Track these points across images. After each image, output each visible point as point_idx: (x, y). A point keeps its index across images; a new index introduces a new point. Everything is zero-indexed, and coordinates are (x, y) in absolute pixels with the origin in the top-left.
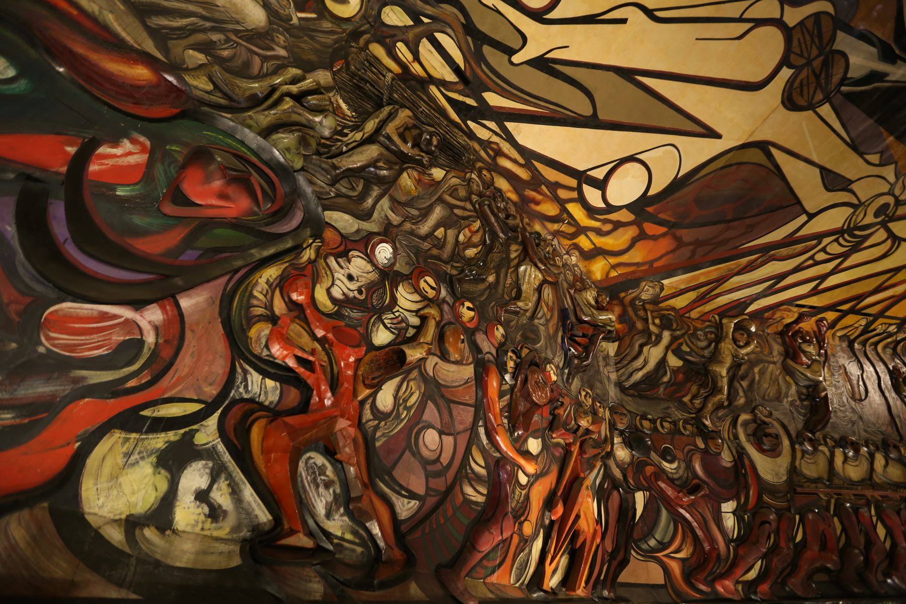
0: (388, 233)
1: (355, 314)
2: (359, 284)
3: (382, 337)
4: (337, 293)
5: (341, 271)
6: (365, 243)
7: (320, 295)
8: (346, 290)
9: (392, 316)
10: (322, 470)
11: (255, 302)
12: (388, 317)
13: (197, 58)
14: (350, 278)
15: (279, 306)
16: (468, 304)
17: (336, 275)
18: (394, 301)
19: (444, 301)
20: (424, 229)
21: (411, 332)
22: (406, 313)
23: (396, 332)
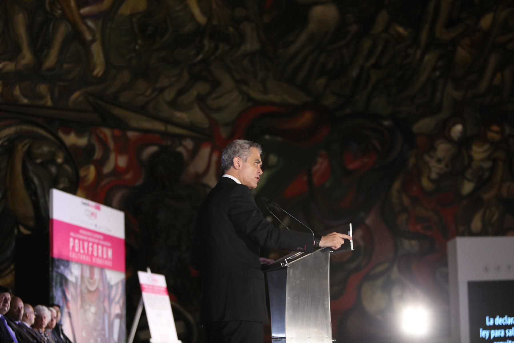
0: (457, 116)
3: (468, 187)
6: (442, 131)
7: (425, 183)
12: (468, 175)
13: (322, 81)
15: (406, 201)
18: (471, 159)
20: (484, 85)
21: (487, 174)
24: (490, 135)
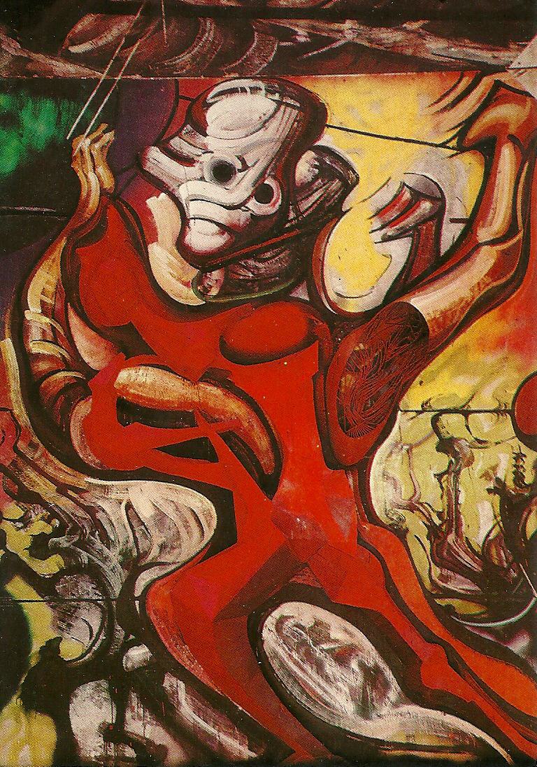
2: (252, 174)
4: (204, 238)
5: (193, 171)
8: (223, 216)
10: (318, 632)
11: (43, 366)
14: (223, 173)
17: (183, 193)
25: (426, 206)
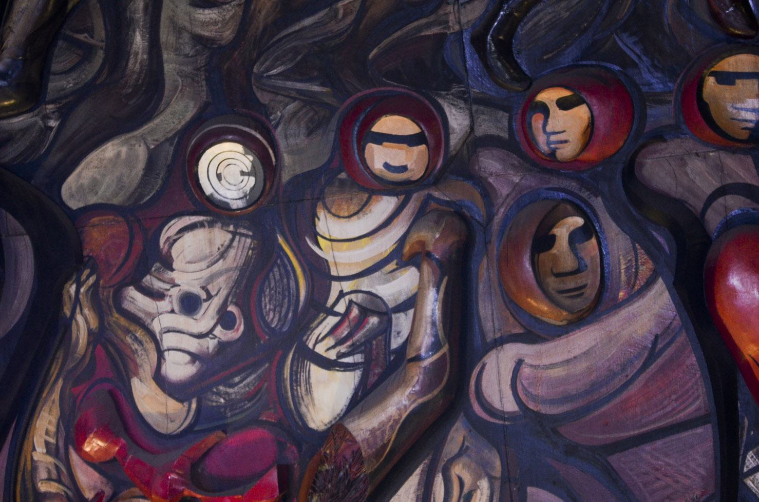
1: (242, 386)
2: (216, 302)
4: (178, 368)
5: (164, 305)
8: (193, 345)
9: (332, 321)
16: (549, 96)
17: (156, 326)
18: (320, 273)
19: (476, 143)
22: (365, 284)
23: (358, 358)
24: (379, 157)
25: (374, 320)
